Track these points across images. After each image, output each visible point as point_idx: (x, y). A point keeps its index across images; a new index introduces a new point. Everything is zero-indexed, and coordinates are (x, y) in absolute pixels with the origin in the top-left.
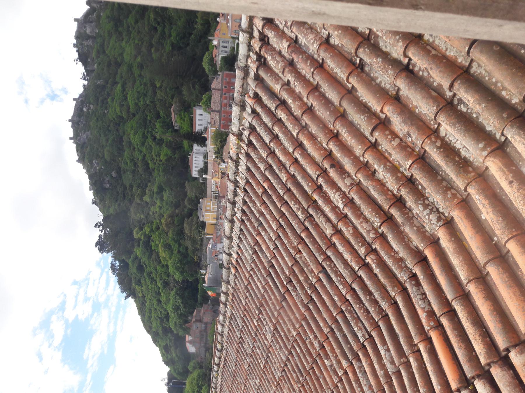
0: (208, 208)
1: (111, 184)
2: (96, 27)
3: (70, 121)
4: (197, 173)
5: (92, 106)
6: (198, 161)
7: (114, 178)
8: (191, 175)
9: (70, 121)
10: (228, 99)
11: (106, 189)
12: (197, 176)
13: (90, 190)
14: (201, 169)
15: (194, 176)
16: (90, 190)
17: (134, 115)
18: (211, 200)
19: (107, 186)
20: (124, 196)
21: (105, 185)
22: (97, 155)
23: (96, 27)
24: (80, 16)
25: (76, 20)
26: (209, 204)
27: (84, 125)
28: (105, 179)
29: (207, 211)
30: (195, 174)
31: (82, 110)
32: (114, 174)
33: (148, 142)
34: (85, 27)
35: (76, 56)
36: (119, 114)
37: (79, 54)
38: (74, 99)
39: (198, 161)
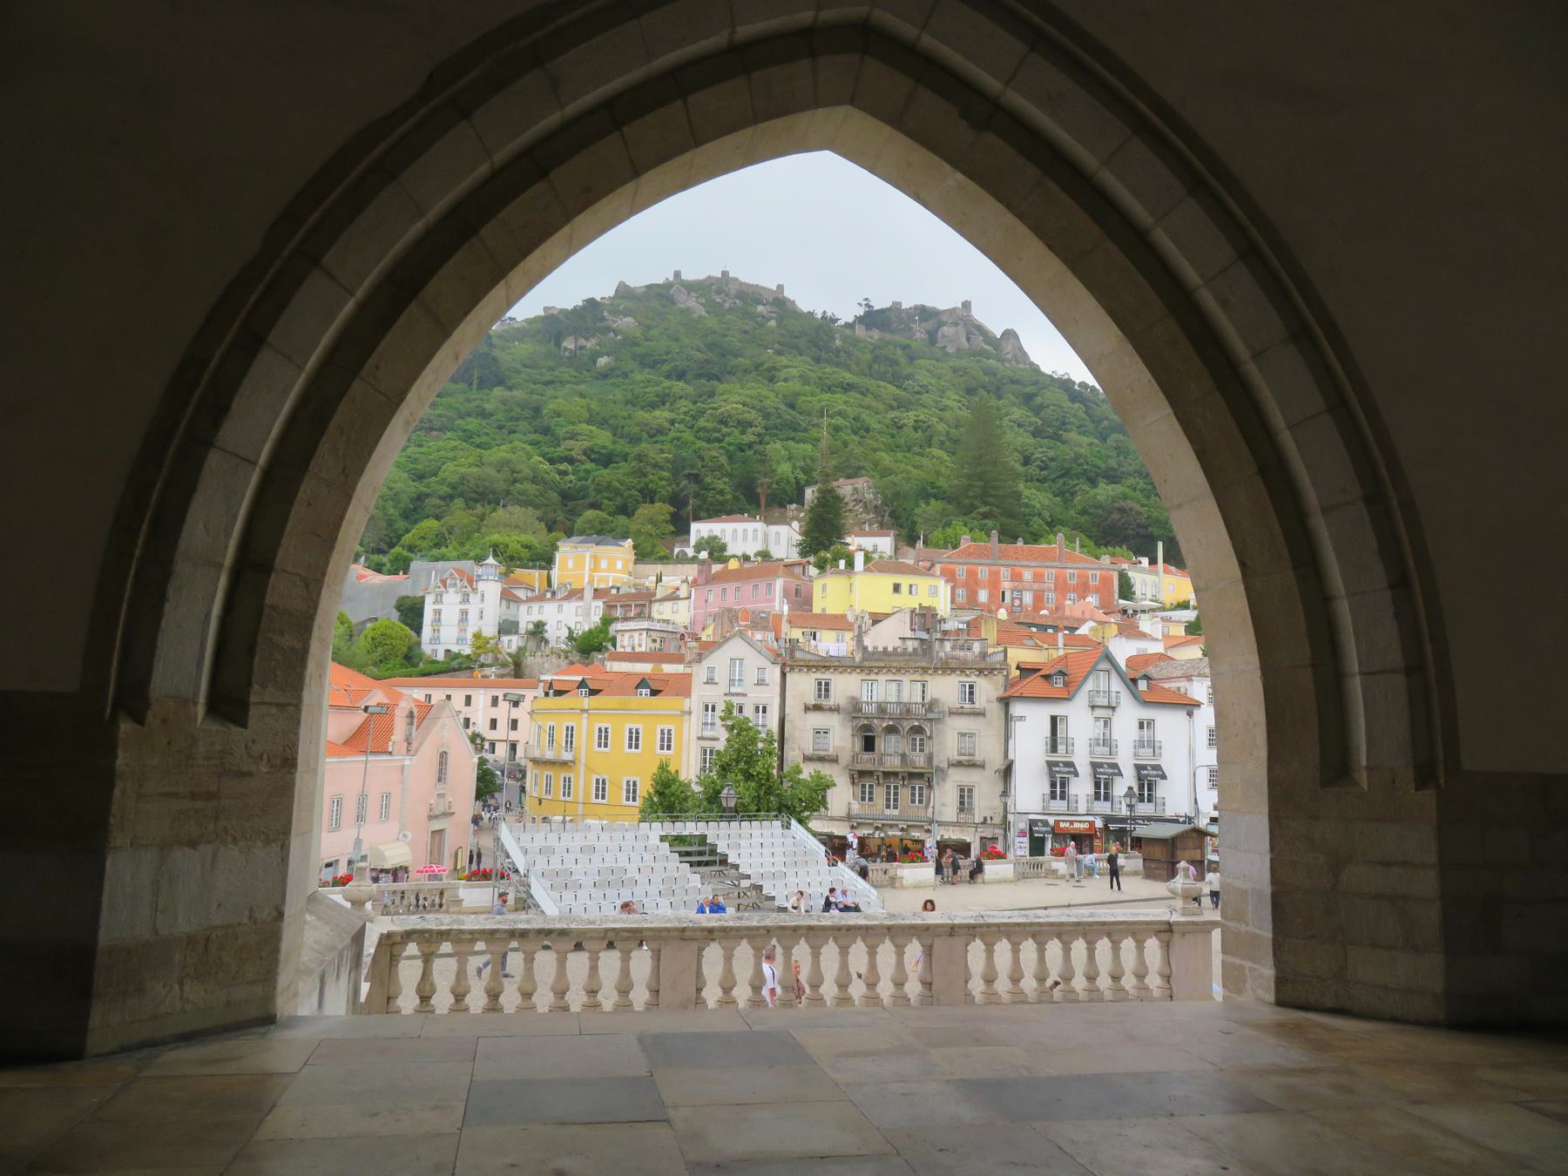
0: (604, 564)
1: (573, 354)
2: (959, 350)
3: (725, 274)
4: (705, 535)
5: (773, 323)
6: (745, 538)
7: (595, 363)
8: (697, 519)
9: (725, 274)
10: (1036, 586)
11: (558, 344)
12: (693, 541)
13: (546, 309)
14: (723, 548)
15: (694, 526)
16: (546, 309)
17: (792, 406)
18: (630, 574)
19: (569, 344)
20: (547, 383)
21: (571, 338)
22: (649, 328)
23: (959, 350)
24: (978, 314)
25: (967, 305)
26: (619, 565)
27: (720, 305)
28: (587, 339)
29: (595, 559)
30: (700, 530)
31: (759, 302)
32: (603, 361)
33: (729, 434)
34: (956, 324)
35: (878, 305)
36: (782, 374)
37: (882, 311)
38: (781, 287)
39: (745, 538)
